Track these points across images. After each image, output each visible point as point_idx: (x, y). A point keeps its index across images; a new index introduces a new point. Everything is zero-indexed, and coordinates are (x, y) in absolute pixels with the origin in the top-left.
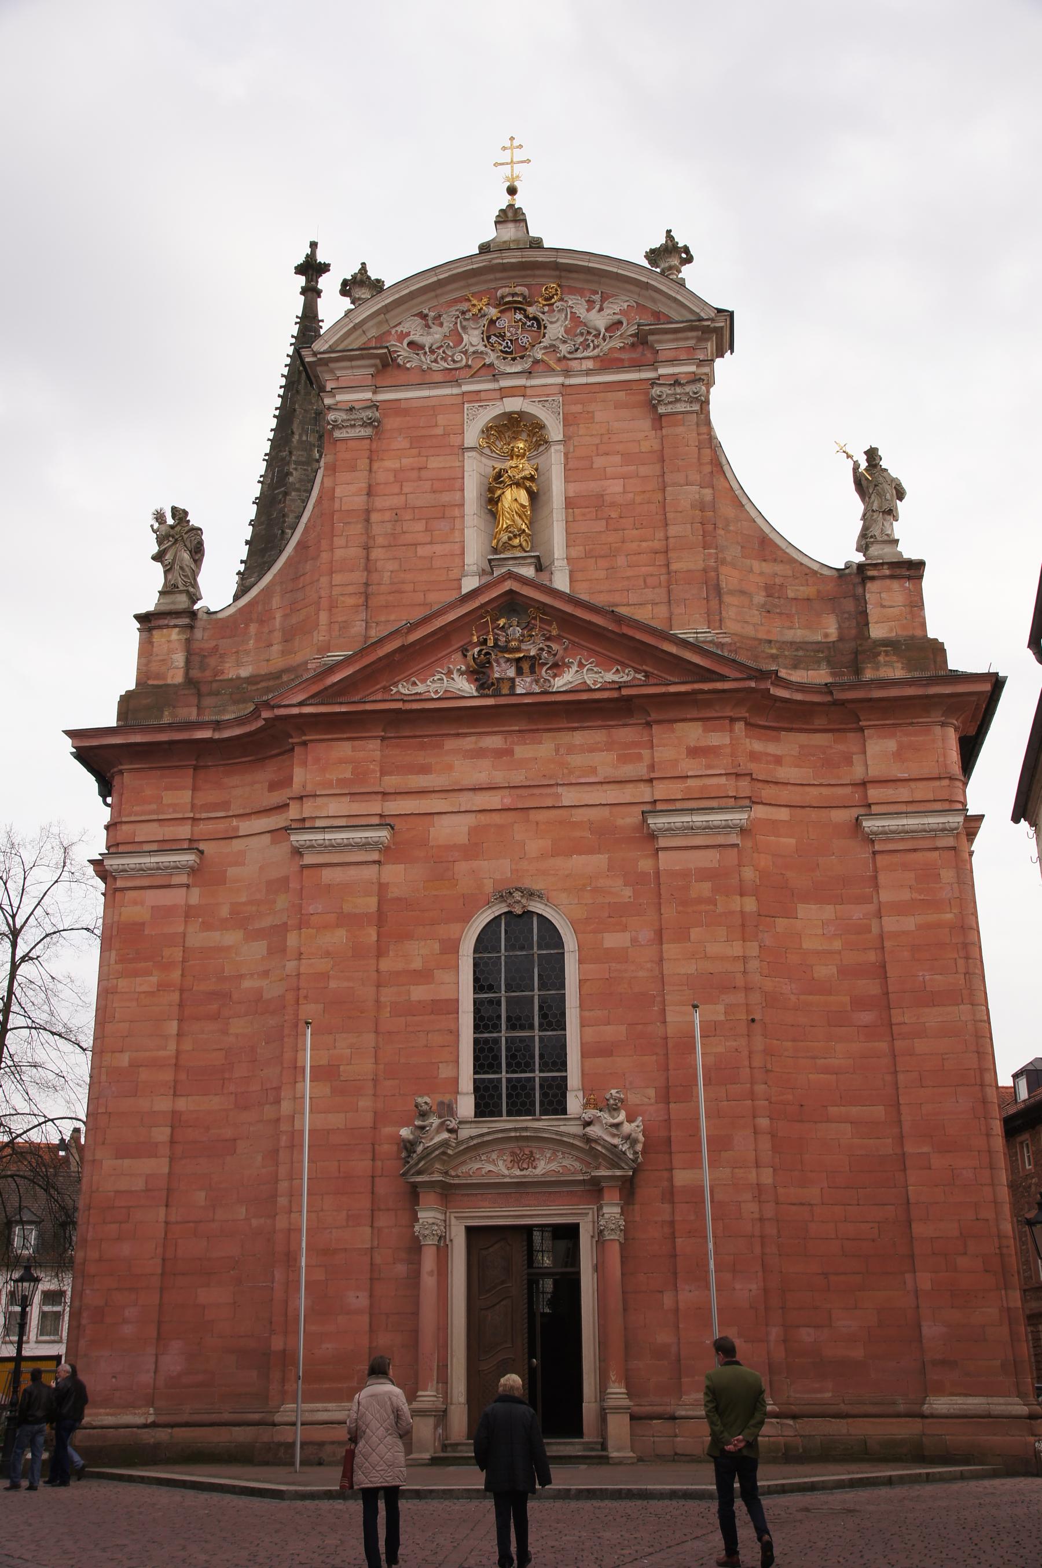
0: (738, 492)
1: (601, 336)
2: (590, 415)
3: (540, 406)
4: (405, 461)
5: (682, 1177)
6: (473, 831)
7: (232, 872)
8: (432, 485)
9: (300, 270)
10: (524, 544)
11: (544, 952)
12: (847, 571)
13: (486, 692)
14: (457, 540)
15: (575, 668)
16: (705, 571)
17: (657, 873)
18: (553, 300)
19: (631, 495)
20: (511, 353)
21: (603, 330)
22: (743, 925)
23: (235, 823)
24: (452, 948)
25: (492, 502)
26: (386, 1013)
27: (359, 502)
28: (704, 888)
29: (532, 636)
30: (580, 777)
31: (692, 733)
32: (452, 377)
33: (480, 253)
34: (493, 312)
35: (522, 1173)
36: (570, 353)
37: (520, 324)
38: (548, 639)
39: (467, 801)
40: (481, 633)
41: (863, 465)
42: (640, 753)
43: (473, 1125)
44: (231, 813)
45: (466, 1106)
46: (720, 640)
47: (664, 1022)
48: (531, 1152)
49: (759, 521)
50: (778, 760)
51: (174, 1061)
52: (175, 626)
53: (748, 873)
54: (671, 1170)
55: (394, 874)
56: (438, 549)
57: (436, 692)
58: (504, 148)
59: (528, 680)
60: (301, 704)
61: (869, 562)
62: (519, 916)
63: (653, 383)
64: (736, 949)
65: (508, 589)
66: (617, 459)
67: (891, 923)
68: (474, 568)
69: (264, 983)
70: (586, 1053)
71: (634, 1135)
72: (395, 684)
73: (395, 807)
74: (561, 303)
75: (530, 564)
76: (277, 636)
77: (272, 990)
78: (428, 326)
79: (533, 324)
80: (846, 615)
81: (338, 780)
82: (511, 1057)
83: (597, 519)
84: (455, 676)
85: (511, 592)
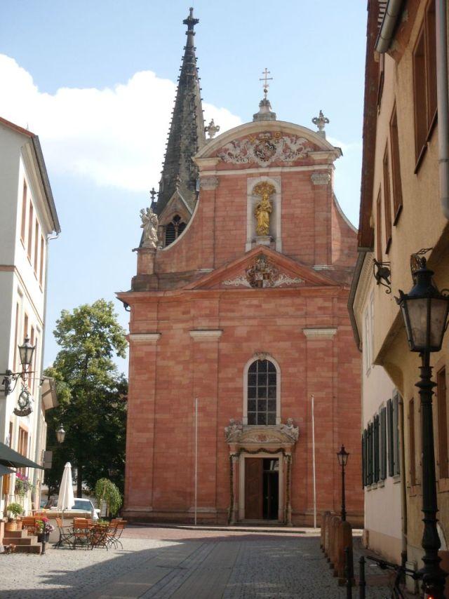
0: (341, 213)
4: (228, 198)
6: (248, 332)
9: (186, 22)
17: (306, 349)
24: (241, 371)
25: (255, 215)
26: (221, 390)
27: (211, 214)
28: (320, 354)
31: (320, 302)
32: (243, 167)
34: (257, 142)
39: (246, 322)
45: (245, 421)
53: (336, 350)
54: (306, 443)
55: (223, 346)
59: (267, 281)
60: (193, 289)
64: (330, 374)
66: (299, 200)
69: (181, 379)
70: (282, 406)
72: (223, 281)
73: (223, 324)
77: (185, 381)
78: (235, 147)
82: (259, 406)
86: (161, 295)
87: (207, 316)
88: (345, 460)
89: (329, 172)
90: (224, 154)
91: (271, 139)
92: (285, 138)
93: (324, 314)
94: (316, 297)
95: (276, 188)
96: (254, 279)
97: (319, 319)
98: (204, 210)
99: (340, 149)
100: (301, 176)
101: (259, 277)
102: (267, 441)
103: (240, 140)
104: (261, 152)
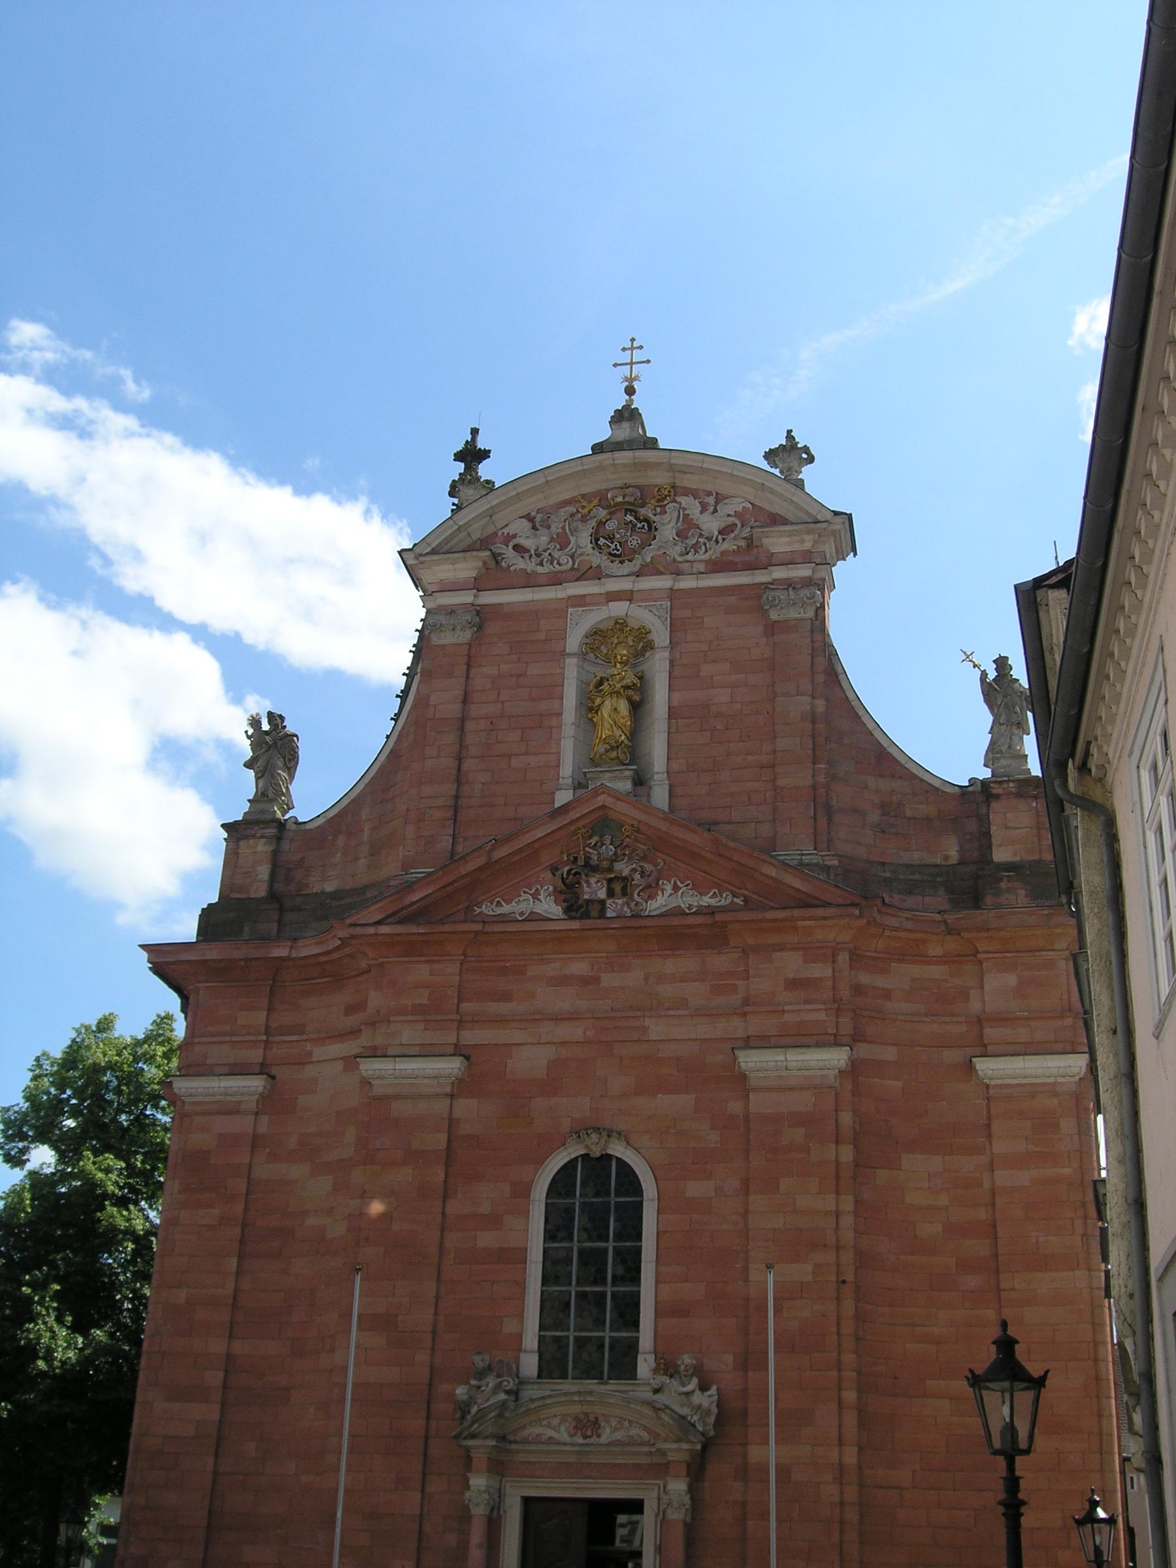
1: (714, 538)
2: (700, 620)
3: (647, 611)
4: (504, 667)
5: (754, 1453)
8: (531, 693)
9: (459, 457)
10: (622, 757)
11: (622, 1199)
12: (971, 789)
13: (574, 914)
14: (554, 751)
15: (669, 889)
16: (814, 787)
17: (747, 1118)
18: (665, 502)
19: (739, 706)
20: (619, 556)
22: (837, 1177)
23: (308, 1048)
24: (523, 1191)
27: (454, 710)
29: (624, 855)
31: (791, 964)
32: (556, 580)
33: (593, 454)
34: (602, 513)
35: (586, 1441)
36: (682, 555)
37: (631, 525)
38: (644, 858)
40: (571, 852)
41: (992, 675)
42: (735, 984)
43: (535, 1386)
44: (305, 1037)
45: (530, 1364)
46: (826, 863)
47: (746, 1280)
48: (597, 1419)
49: (877, 734)
50: (887, 995)
51: (230, 1301)
52: (262, 837)
54: (745, 1445)
55: (466, 1107)
57: (522, 914)
58: (624, 349)
59: (620, 902)
60: (379, 923)
61: (994, 779)
62: (597, 1159)
63: (766, 588)
64: (828, 1203)
65: (600, 804)
67: (1004, 1178)
68: (570, 781)
70: (659, 1313)
71: (705, 1404)
72: (479, 905)
73: (471, 1037)
74: (674, 504)
75: (627, 778)
78: (534, 528)
79: (644, 526)
80: (968, 837)
84: (541, 897)
85: (603, 807)
89: (821, 585)
92: (684, 501)
93: (807, 1002)
94: (782, 948)
95: (654, 636)
97: (787, 1017)
98: (433, 699)
99: (850, 516)
101: (594, 889)
102: (604, 1439)
104: (611, 538)
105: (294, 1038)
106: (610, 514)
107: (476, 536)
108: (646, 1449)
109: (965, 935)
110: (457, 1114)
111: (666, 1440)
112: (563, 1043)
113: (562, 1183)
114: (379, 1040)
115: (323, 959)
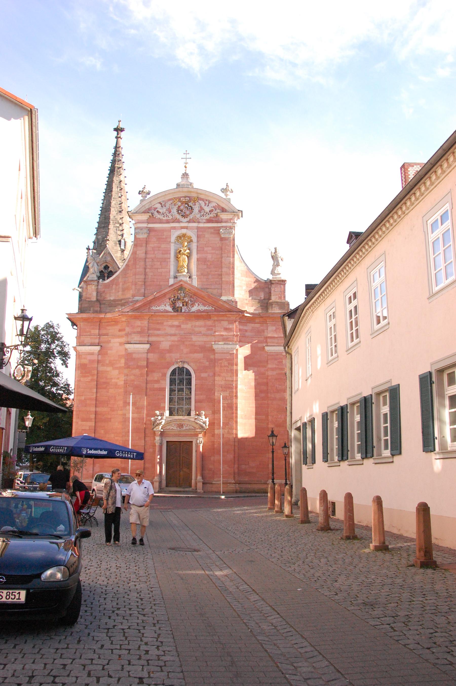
6: (171, 346)
7: (109, 352)
13: (174, 310)
15: (197, 305)
17: (215, 359)
20: (184, 216)
21: (208, 212)
24: (164, 375)
25: (177, 258)
26: (148, 390)
27: (143, 255)
30: (197, 334)
32: (168, 222)
34: (179, 204)
38: (191, 297)
39: (169, 338)
48: (182, 425)
55: (151, 356)
56: (163, 270)
57: (162, 309)
59: (185, 307)
61: (273, 279)
66: (210, 248)
67: (270, 373)
70: (196, 402)
73: (152, 339)
76: (120, 290)
78: (162, 206)
81: (137, 331)
83: (205, 265)
84: (167, 306)
86: (102, 316)
87: (138, 332)
88: (274, 441)
90: (153, 211)
91: (190, 202)
92: (201, 202)
95: (192, 238)
96: (175, 306)
98: (138, 252)
100: (212, 230)
101: (179, 304)
103: (165, 202)
104: (182, 211)
105: (106, 337)
106: (181, 204)
107: (147, 207)
108: (193, 431)
109: (264, 318)
110: (148, 357)
111: (197, 429)
112: (172, 341)
113: (173, 373)
114: (129, 340)
115: (113, 318)
